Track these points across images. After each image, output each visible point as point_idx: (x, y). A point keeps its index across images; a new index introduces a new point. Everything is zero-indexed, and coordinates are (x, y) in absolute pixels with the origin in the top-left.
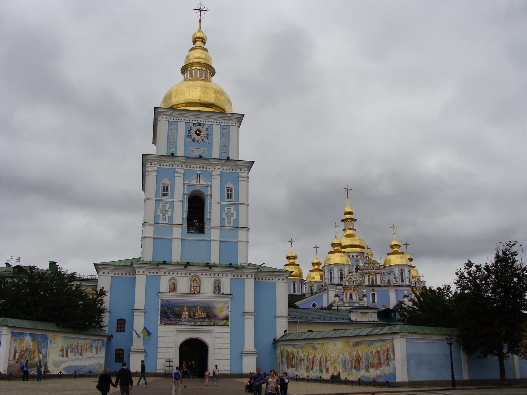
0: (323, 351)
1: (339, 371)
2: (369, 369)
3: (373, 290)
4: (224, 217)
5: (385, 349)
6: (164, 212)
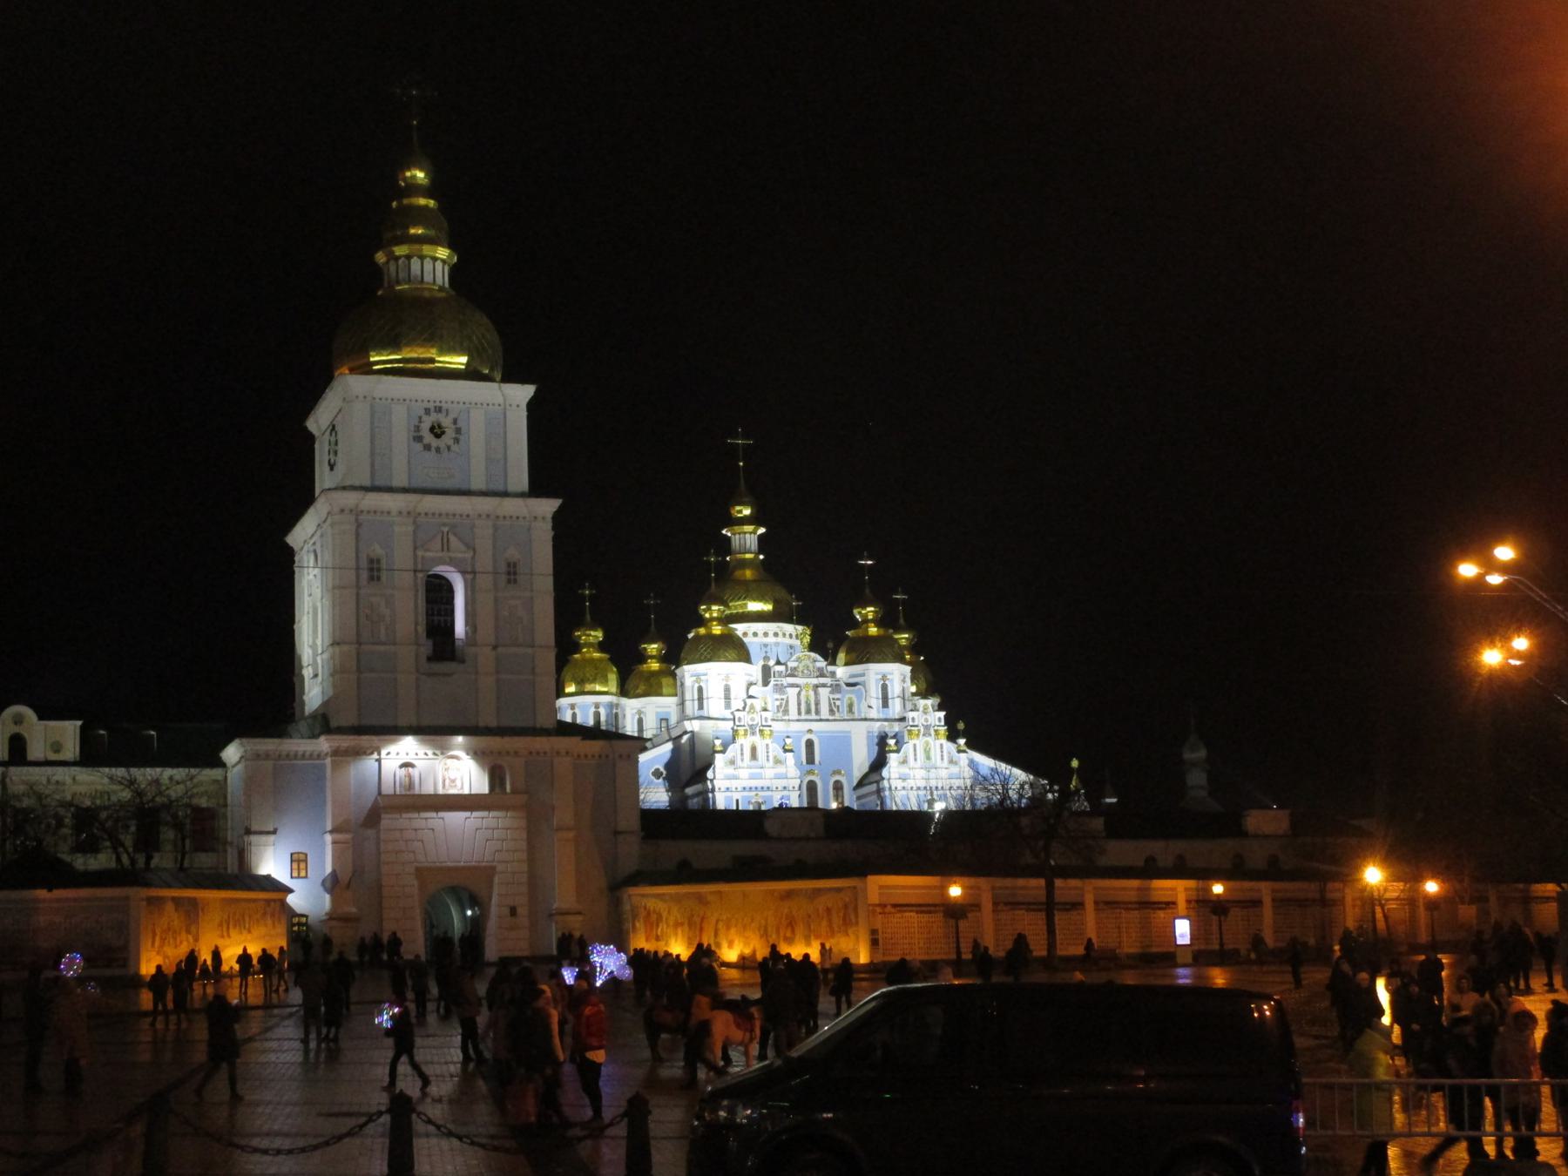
3: (810, 731)
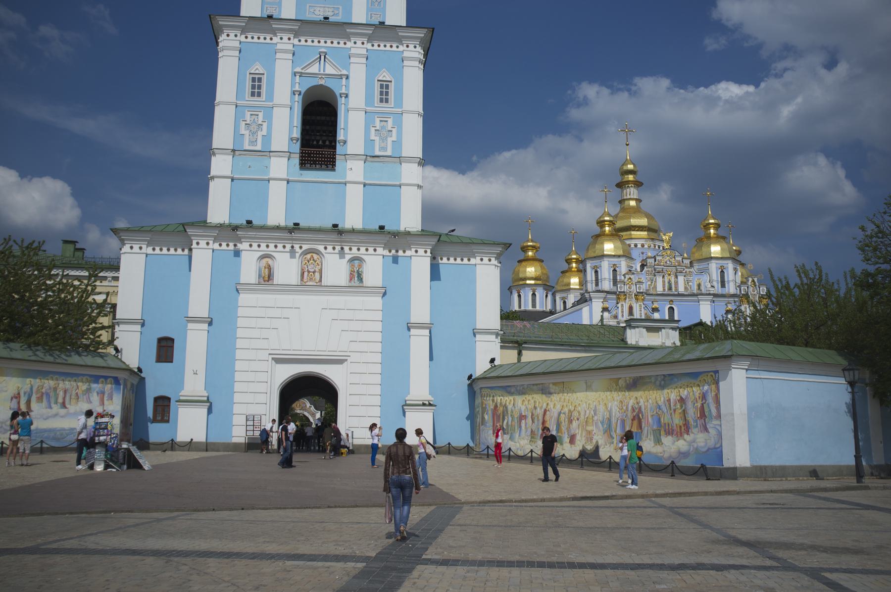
0: (564, 399)
1: (597, 442)
2: (662, 437)
3: (672, 301)
4: (373, 137)
5: (697, 395)
6: (254, 127)
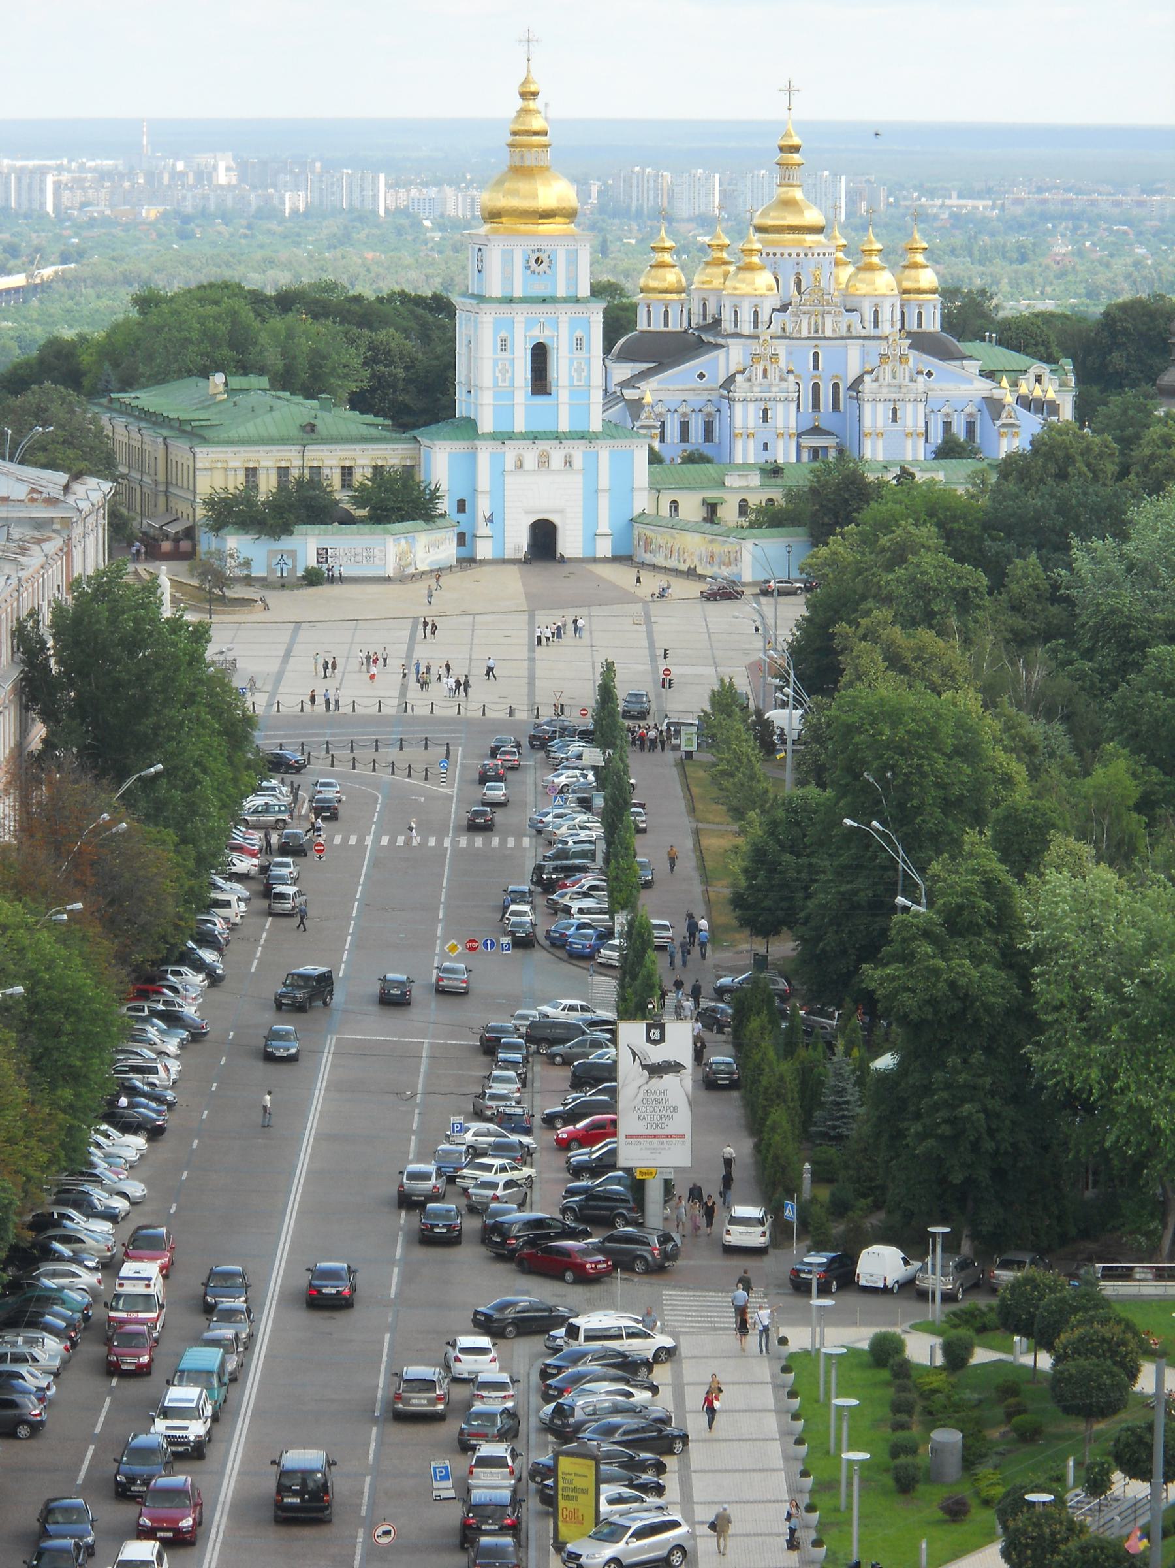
3: (816, 346)
